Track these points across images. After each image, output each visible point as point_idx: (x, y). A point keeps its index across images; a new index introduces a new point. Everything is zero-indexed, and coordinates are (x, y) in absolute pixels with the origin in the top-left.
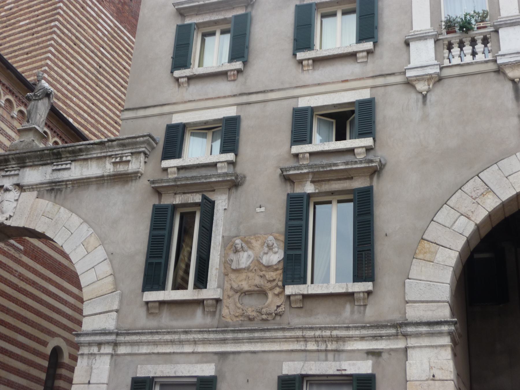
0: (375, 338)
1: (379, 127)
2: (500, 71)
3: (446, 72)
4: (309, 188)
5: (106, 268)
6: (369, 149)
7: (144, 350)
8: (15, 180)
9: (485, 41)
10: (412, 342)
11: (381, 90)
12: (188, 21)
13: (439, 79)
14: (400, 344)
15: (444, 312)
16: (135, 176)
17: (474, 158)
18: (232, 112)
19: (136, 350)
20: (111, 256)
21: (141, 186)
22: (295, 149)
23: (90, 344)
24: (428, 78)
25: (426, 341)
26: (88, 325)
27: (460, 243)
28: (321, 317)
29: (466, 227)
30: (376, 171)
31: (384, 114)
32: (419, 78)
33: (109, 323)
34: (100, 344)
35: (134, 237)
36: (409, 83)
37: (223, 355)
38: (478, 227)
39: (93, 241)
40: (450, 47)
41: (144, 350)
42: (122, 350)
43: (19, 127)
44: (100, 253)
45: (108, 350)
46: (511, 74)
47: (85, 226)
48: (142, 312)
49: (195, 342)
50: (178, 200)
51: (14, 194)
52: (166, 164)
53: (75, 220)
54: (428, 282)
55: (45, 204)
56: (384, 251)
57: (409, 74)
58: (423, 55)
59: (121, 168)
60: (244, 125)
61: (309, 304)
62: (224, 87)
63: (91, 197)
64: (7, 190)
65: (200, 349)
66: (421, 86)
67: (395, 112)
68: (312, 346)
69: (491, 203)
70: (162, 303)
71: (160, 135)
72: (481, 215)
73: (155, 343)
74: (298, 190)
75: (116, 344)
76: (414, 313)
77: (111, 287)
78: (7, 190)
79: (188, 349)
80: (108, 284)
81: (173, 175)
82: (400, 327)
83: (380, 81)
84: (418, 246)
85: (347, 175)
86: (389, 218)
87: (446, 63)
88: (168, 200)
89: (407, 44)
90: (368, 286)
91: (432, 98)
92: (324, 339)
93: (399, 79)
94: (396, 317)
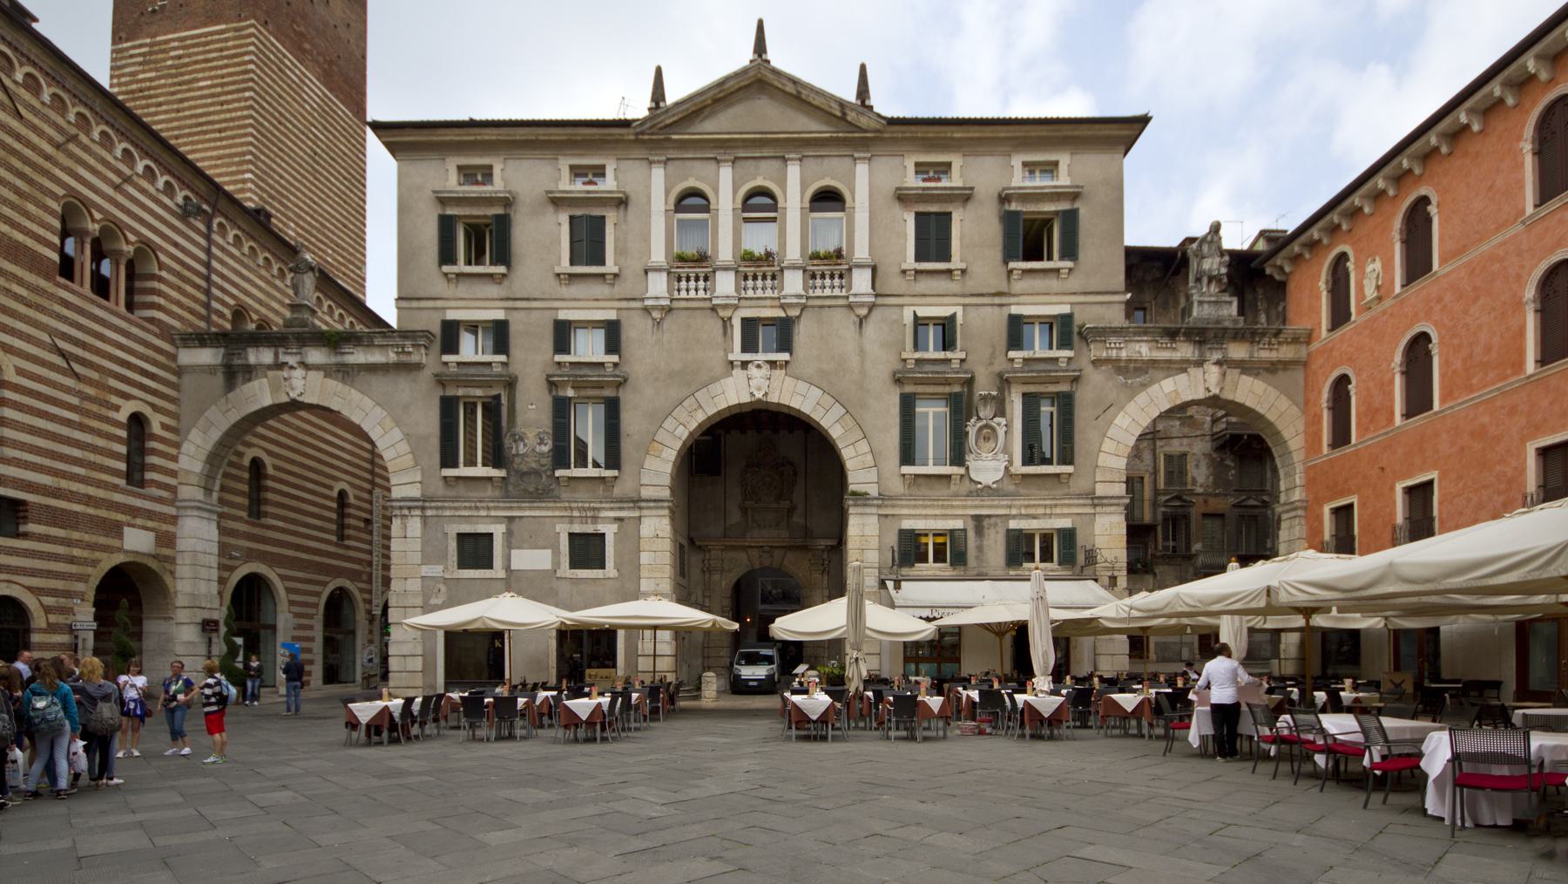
0: (621, 509)
1: (623, 345)
2: (714, 309)
3: (676, 304)
4: (570, 393)
5: (404, 447)
6: (616, 365)
7: (448, 513)
8: (298, 358)
9: (706, 279)
10: (645, 512)
11: (624, 313)
12: (450, 212)
13: (670, 310)
14: (637, 514)
15: (666, 493)
16: (418, 367)
17: (694, 380)
18: (500, 315)
19: (440, 512)
20: (407, 436)
21: (427, 374)
22: (558, 358)
23: (401, 508)
24: (662, 308)
25: (654, 512)
26: (396, 493)
27: (679, 445)
28: (582, 494)
29: (683, 433)
30: (621, 384)
31: (629, 334)
32: (654, 308)
33: (415, 492)
34: (410, 508)
35: (429, 422)
36: (647, 310)
37: (511, 519)
38: (691, 434)
39: (389, 422)
40: (679, 280)
41: (448, 513)
42: (429, 513)
43: (287, 301)
44: (397, 434)
45: (418, 512)
46: (722, 313)
47: (378, 409)
48: (441, 484)
49: (488, 508)
50: (460, 392)
51: (299, 373)
52: (446, 358)
53: (368, 403)
54: (656, 469)
55: (333, 385)
56: (627, 446)
57: (648, 303)
58: (658, 286)
59: (404, 358)
60: (513, 329)
61: (573, 484)
62: (492, 290)
63: (379, 383)
64: (292, 368)
65: (493, 513)
66: (656, 315)
67: (635, 330)
68: (576, 514)
69: (701, 417)
70: (458, 478)
71: (436, 329)
72: (693, 425)
73: (456, 509)
74: (561, 393)
75: (423, 508)
76: (646, 493)
77: (412, 463)
78: (292, 368)
79: (483, 513)
80: (408, 460)
81: (453, 369)
82: (636, 502)
83: (624, 304)
84: (649, 444)
85: (600, 386)
86: (631, 422)
87: (676, 295)
88: (451, 392)
89: (646, 272)
90: (615, 473)
91: (665, 325)
92: (584, 509)
93: (638, 304)
94: (634, 495)
